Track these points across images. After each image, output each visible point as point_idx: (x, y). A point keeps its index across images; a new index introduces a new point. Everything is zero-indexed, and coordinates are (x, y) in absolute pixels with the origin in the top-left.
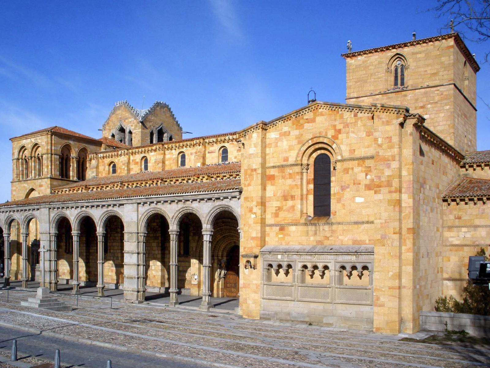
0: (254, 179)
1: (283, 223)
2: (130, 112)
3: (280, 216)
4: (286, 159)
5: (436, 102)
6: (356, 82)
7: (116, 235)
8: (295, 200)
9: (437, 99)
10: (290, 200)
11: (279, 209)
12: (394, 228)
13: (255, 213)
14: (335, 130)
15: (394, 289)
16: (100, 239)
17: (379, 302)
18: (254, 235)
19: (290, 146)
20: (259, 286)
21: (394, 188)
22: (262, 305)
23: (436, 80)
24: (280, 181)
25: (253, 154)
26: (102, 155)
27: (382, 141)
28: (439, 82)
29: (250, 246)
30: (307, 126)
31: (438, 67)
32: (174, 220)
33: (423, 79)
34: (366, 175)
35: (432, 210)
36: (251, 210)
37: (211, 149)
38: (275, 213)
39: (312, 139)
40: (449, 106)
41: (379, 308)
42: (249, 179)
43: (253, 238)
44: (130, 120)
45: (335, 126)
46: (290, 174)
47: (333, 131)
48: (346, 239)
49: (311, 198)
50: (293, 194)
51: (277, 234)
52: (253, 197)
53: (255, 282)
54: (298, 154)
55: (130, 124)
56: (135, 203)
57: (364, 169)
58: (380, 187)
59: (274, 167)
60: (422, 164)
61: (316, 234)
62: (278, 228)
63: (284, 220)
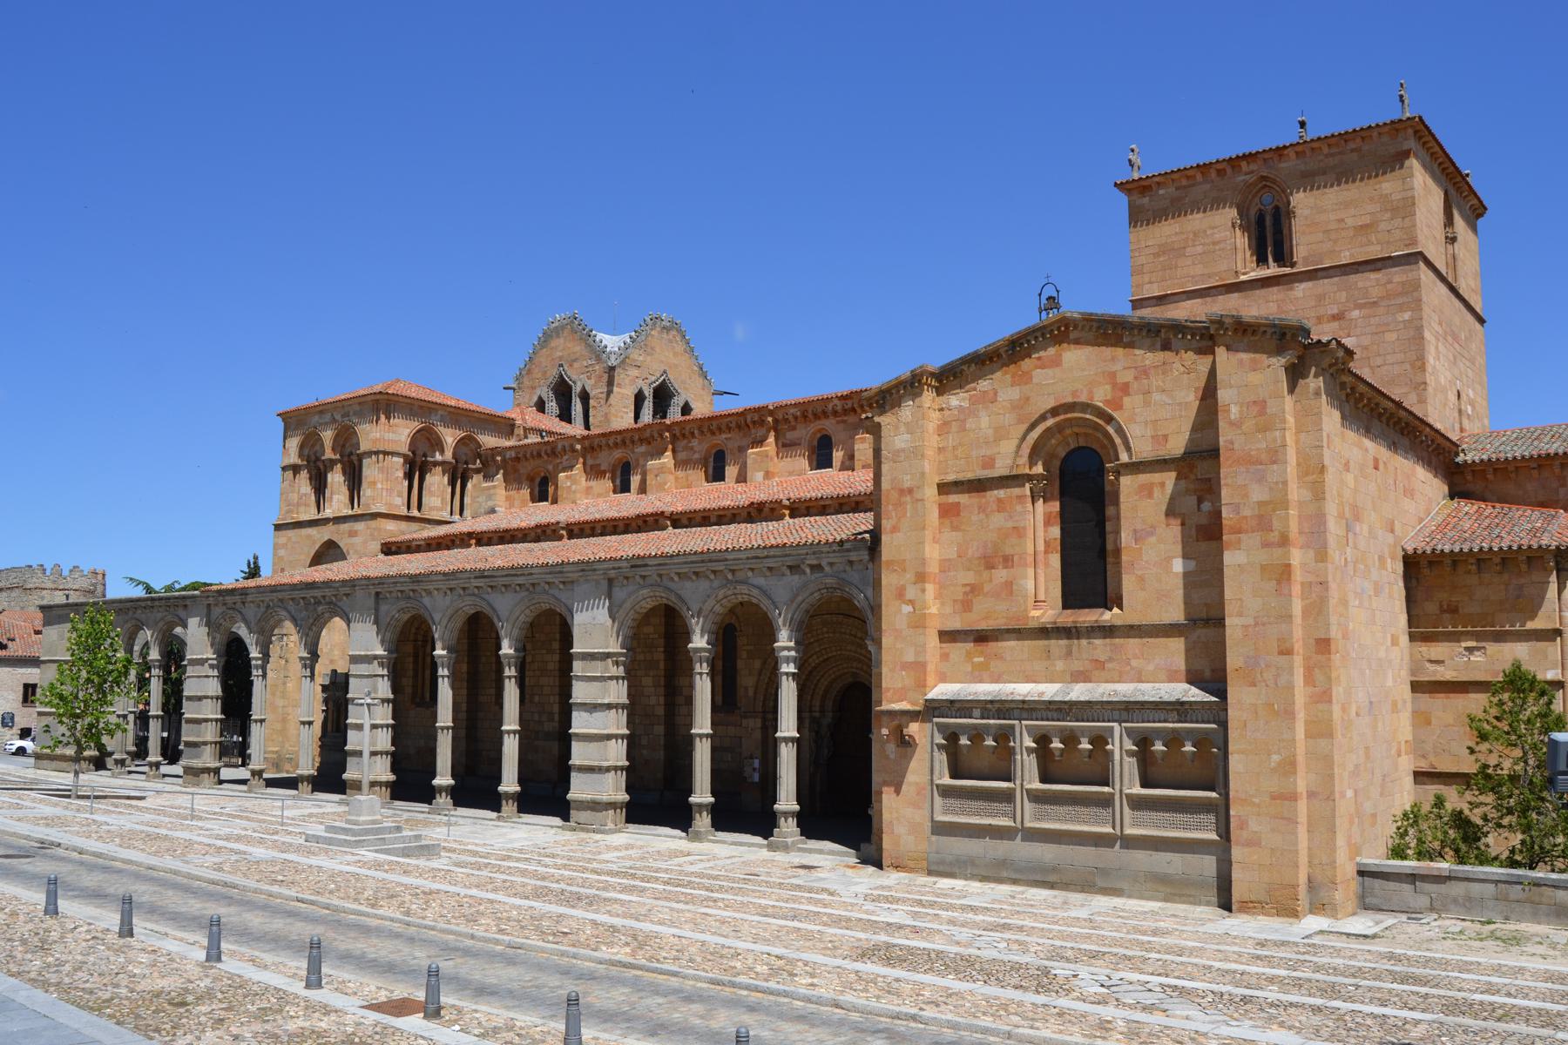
0: (908, 515)
2: (586, 340)
4: (989, 462)
5: (1374, 303)
6: (1156, 255)
8: (1013, 566)
9: (1375, 293)
11: (974, 589)
12: (1278, 640)
13: (910, 601)
14: (1114, 385)
15: (1286, 799)
17: (1245, 834)
21: (1276, 533)
23: (1370, 243)
24: (974, 518)
25: (903, 450)
27: (1241, 412)
28: (1378, 248)
30: (1039, 375)
31: (1371, 208)
33: (1335, 241)
34: (1200, 501)
35: (1377, 592)
36: (900, 594)
40: (1410, 313)
41: (1246, 850)
42: (893, 514)
43: (905, 666)
45: (1113, 375)
46: (1000, 500)
47: (1108, 387)
48: (1151, 667)
49: (1055, 560)
50: (1008, 551)
51: (969, 655)
54: (1019, 447)
57: (1192, 486)
58: (1240, 532)
60: (1348, 470)
61: (1069, 653)
63: (987, 618)
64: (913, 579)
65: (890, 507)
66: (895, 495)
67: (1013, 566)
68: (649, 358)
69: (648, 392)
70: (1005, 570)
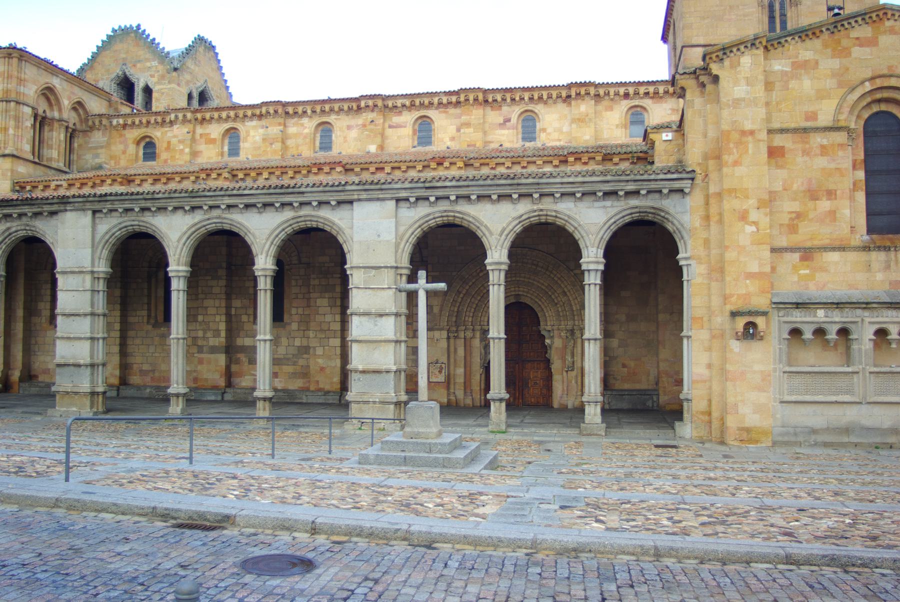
0: (750, 151)
1: (809, 244)
3: (800, 231)
4: (813, 116)
7: (214, 283)
8: (836, 199)
10: (824, 199)
13: (754, 222)
16: (265, 285)
18: (754, 268)
19: (818, 91)
20: (769, 375)
22: (778, 416)
24: (799, 159)
25: (744, 100)
26: (121, 121)
29: (743, 291)
30: (857, 52)
32: (503, 237)
36: (743, 217)
37: (396, 119)
38: (788, 225)
39: (873, 79)
42: (735, 151)
43: (750, 276)
44: (148, 64)
46: (823, 147)
50: (832, 187)
51: (795, 268)
52: (747, 189)
53: (757, 368)
55: (150, 73)
56: (392, 199)
59: (782, 131)
62: (796, 256)
63: (811, 239)
64: (756, 205)
65: (732, 145)
66: (735, 136)
67: (836, 199)
68: (197, 69)
69: (195, 95)
70: (829, 202)
